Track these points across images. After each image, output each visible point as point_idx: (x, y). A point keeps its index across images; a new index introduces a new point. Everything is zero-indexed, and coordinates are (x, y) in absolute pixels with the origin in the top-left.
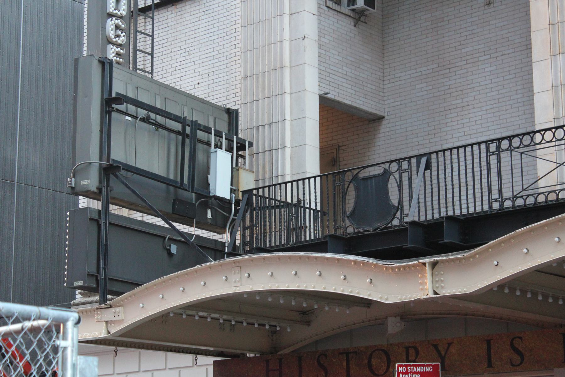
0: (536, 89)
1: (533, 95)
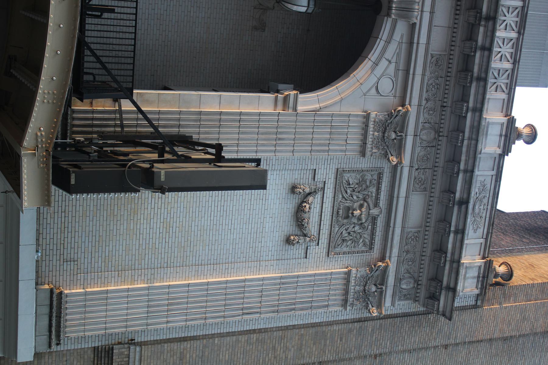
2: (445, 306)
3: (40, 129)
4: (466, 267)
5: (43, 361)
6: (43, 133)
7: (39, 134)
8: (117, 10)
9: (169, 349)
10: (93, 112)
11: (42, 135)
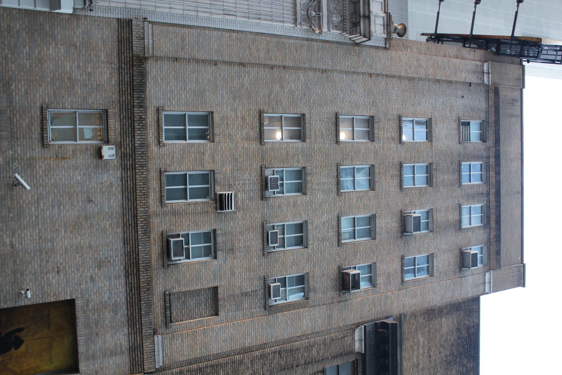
2: (365, 30)
4: (375, 16)
5: (80, 22)
9: (173, 31)
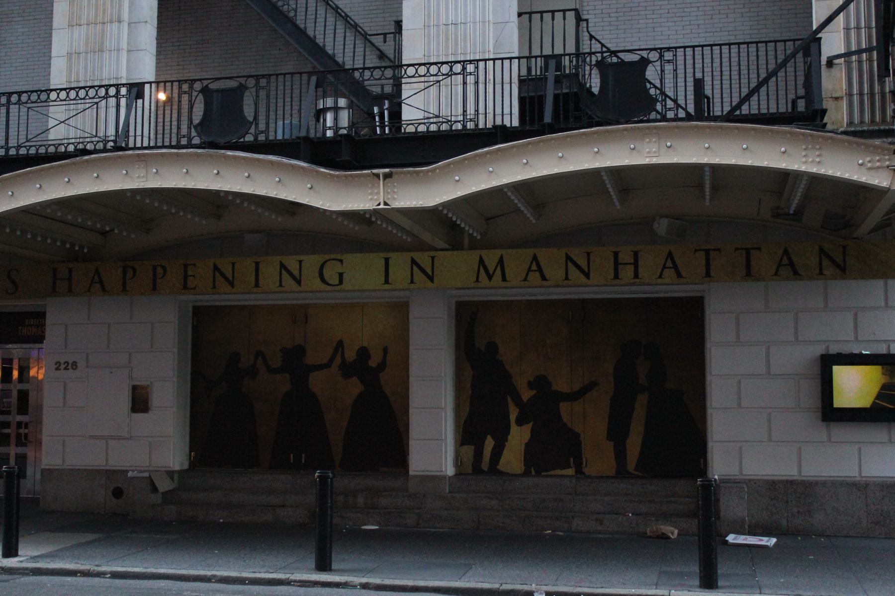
0: (53, 54)
1: (50, 59)
3: (861, 165)
6: (868, 159)
7: (869, 165)
8: (699, 75)
10: (850, 95)
11: (869, 162)
